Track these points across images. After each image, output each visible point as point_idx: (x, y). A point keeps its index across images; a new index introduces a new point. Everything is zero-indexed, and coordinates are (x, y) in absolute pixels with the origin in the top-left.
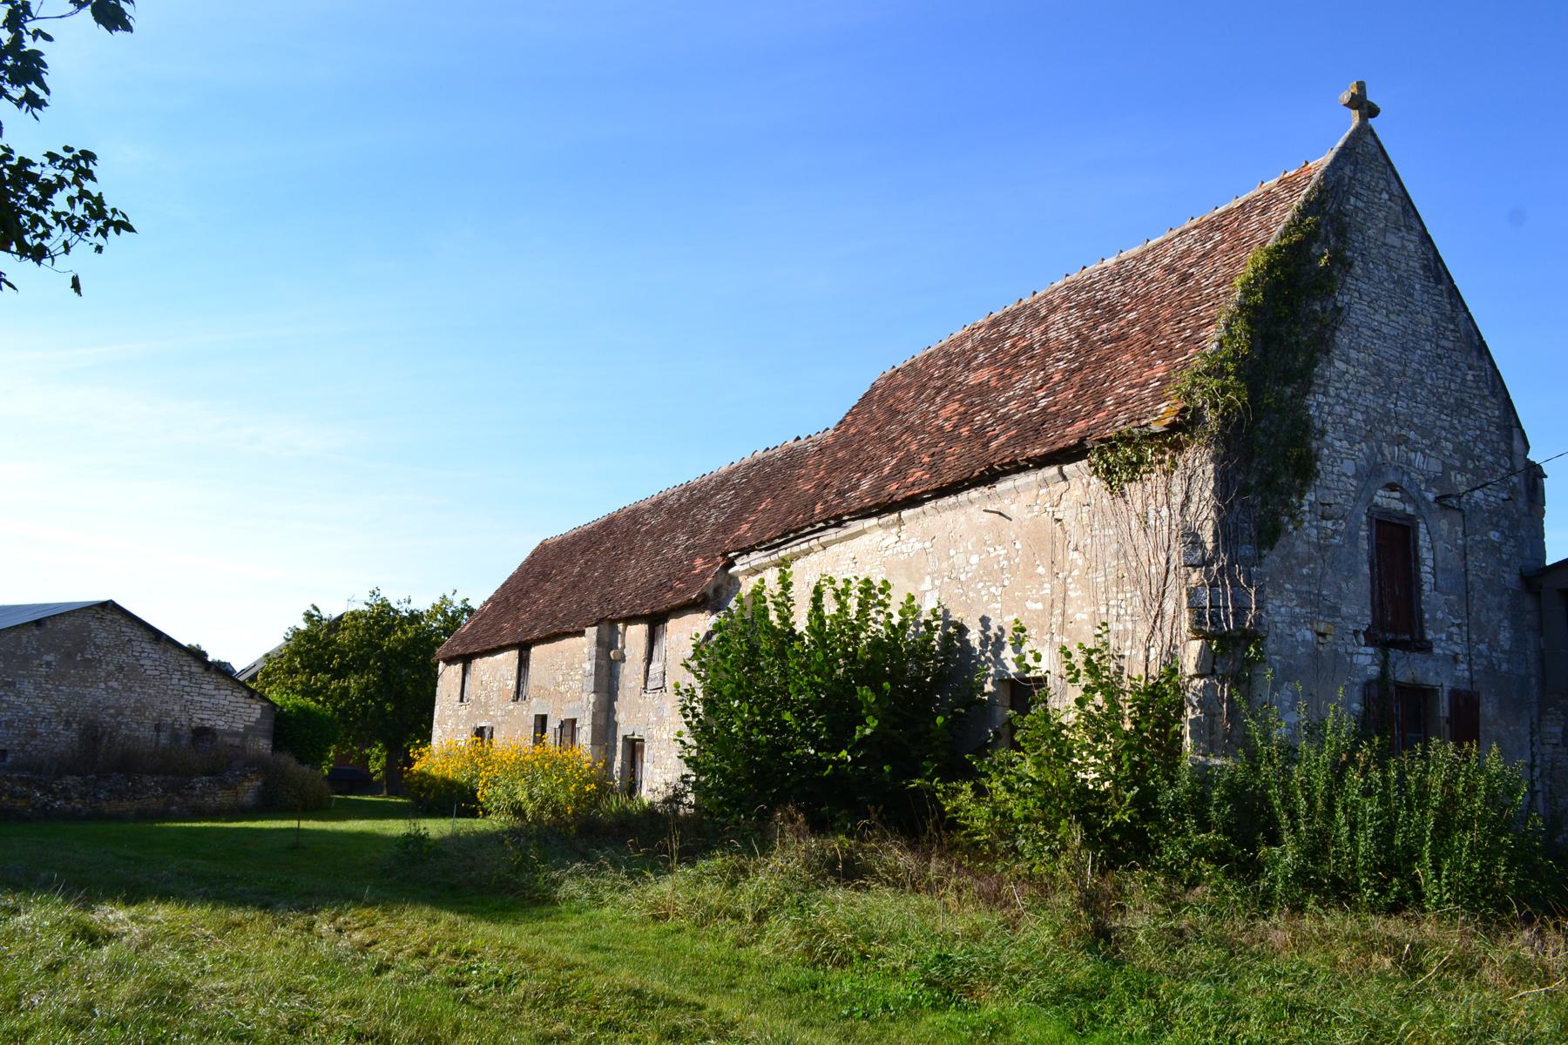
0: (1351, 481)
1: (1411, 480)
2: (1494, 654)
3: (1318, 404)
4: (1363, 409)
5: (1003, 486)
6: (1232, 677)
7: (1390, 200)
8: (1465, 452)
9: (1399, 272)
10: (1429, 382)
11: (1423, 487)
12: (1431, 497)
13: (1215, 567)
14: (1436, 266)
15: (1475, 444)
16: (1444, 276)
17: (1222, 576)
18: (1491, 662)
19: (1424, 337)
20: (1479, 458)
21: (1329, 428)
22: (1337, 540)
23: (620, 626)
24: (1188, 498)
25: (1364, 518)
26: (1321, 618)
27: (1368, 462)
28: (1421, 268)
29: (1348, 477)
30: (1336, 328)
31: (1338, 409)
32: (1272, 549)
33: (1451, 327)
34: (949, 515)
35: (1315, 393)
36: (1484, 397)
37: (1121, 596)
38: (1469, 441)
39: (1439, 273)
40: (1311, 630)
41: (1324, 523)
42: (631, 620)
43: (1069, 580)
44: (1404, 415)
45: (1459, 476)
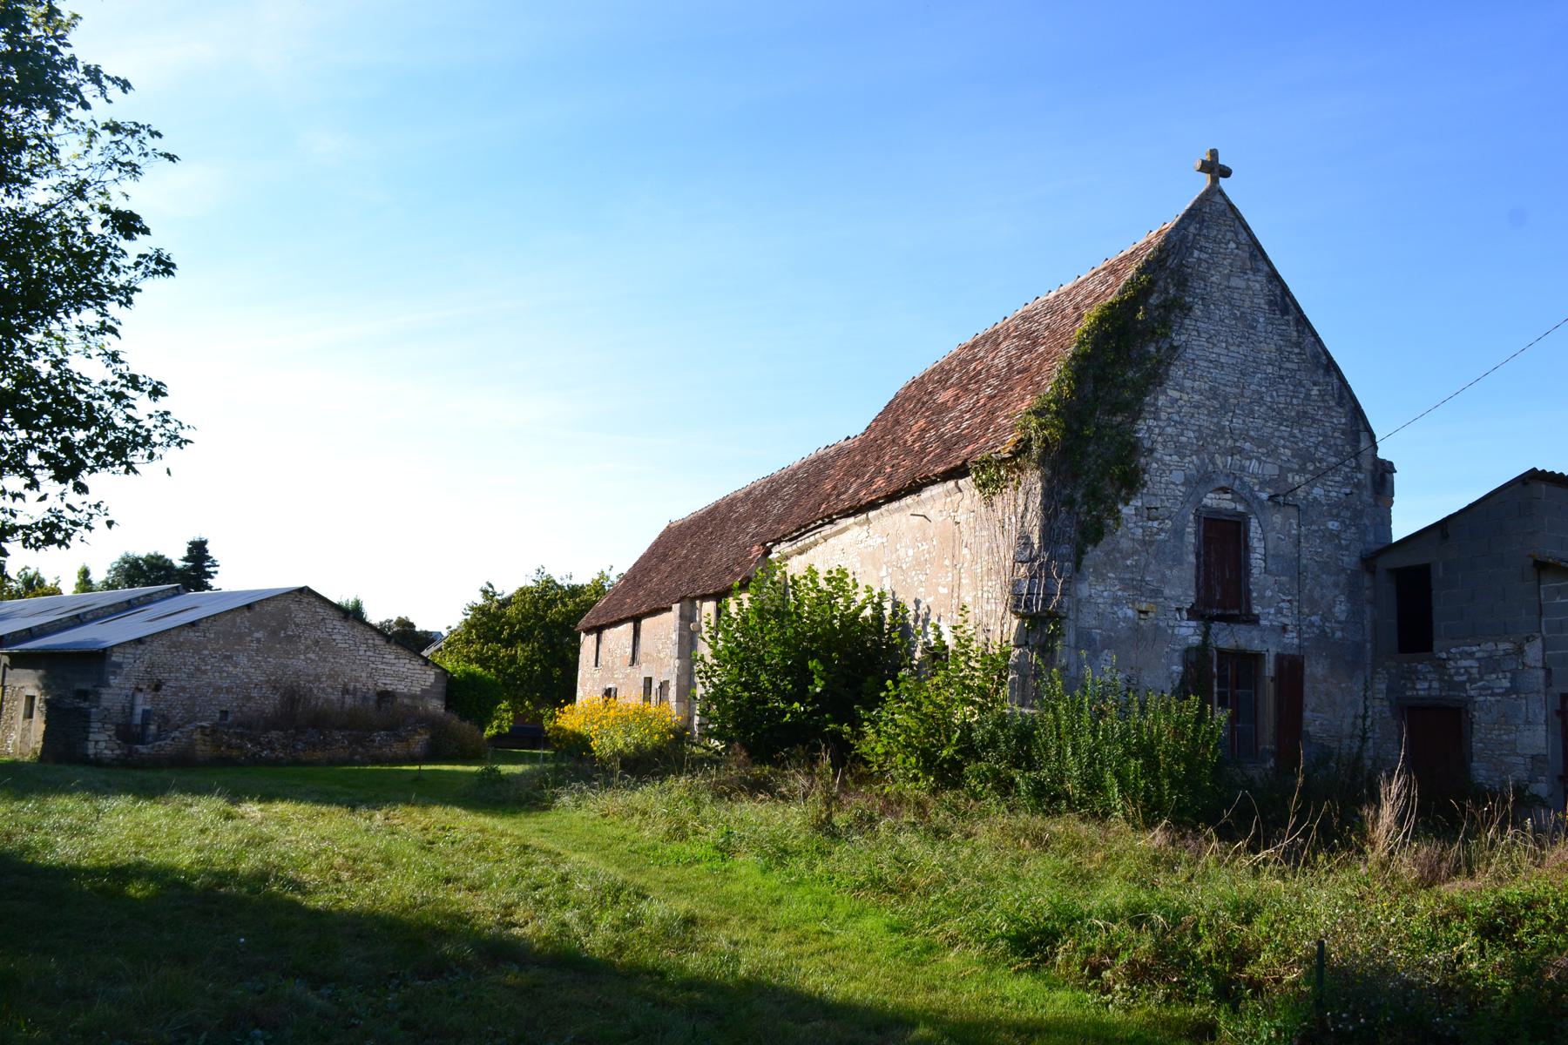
0: (1179, 487)
1: (1243, 483)
2: (1327, 624)
3: (1149, 427)
4: (1196, 428)
5: (927, 493)
6: (1039, 647)
7: (1237, 248)
8: (1305, 457)
9: (1242, 309)
10: (1269, 399)
11: (1256, 488)
12: (1264, 496)
13: (1037, 564)
14: (1283, 299)
15: (1316, 449)
16: (1292, 307)
17: (1041, 570)
18: (1323, 631)
19: (1265, 362)
20: (1321, 460)
21: (1159, 447)
22: (1163, 536)
23: (698, 602)
24: (1026, 509)
25: (1192, 517)
26: (1143, 599)
27: (1198, 472)
28: (1266, 304)
29: (1177, 485)
30: (1170, 364)
31: (1169, 430)
32: (1095, 546)
33: (1297, 350)
34: (896, 516)
35: (1145, 419)
36: (1330, 408)
37: (990, 584)
38: (1310, 447)
39: (1286, 305)
40: (1132, 609)
41: (1150, 523)
42: (705, 598)
43: (962, 571)
44: (1239, 429)
45: (1297, 478)
